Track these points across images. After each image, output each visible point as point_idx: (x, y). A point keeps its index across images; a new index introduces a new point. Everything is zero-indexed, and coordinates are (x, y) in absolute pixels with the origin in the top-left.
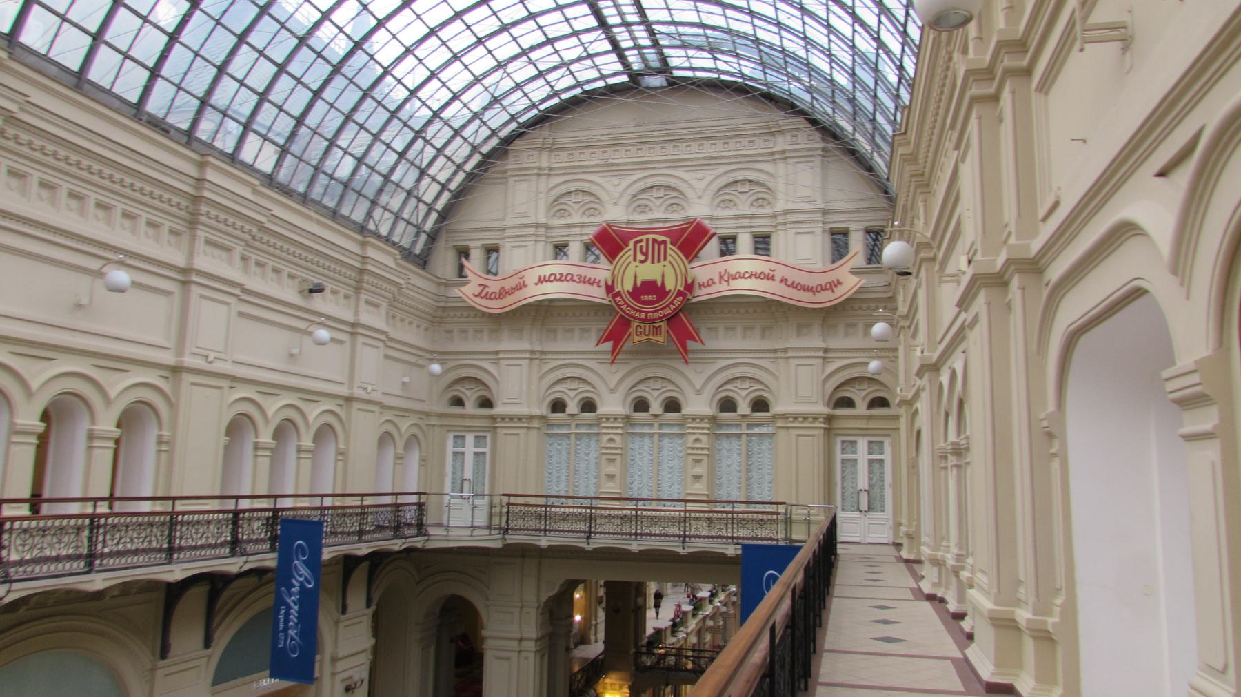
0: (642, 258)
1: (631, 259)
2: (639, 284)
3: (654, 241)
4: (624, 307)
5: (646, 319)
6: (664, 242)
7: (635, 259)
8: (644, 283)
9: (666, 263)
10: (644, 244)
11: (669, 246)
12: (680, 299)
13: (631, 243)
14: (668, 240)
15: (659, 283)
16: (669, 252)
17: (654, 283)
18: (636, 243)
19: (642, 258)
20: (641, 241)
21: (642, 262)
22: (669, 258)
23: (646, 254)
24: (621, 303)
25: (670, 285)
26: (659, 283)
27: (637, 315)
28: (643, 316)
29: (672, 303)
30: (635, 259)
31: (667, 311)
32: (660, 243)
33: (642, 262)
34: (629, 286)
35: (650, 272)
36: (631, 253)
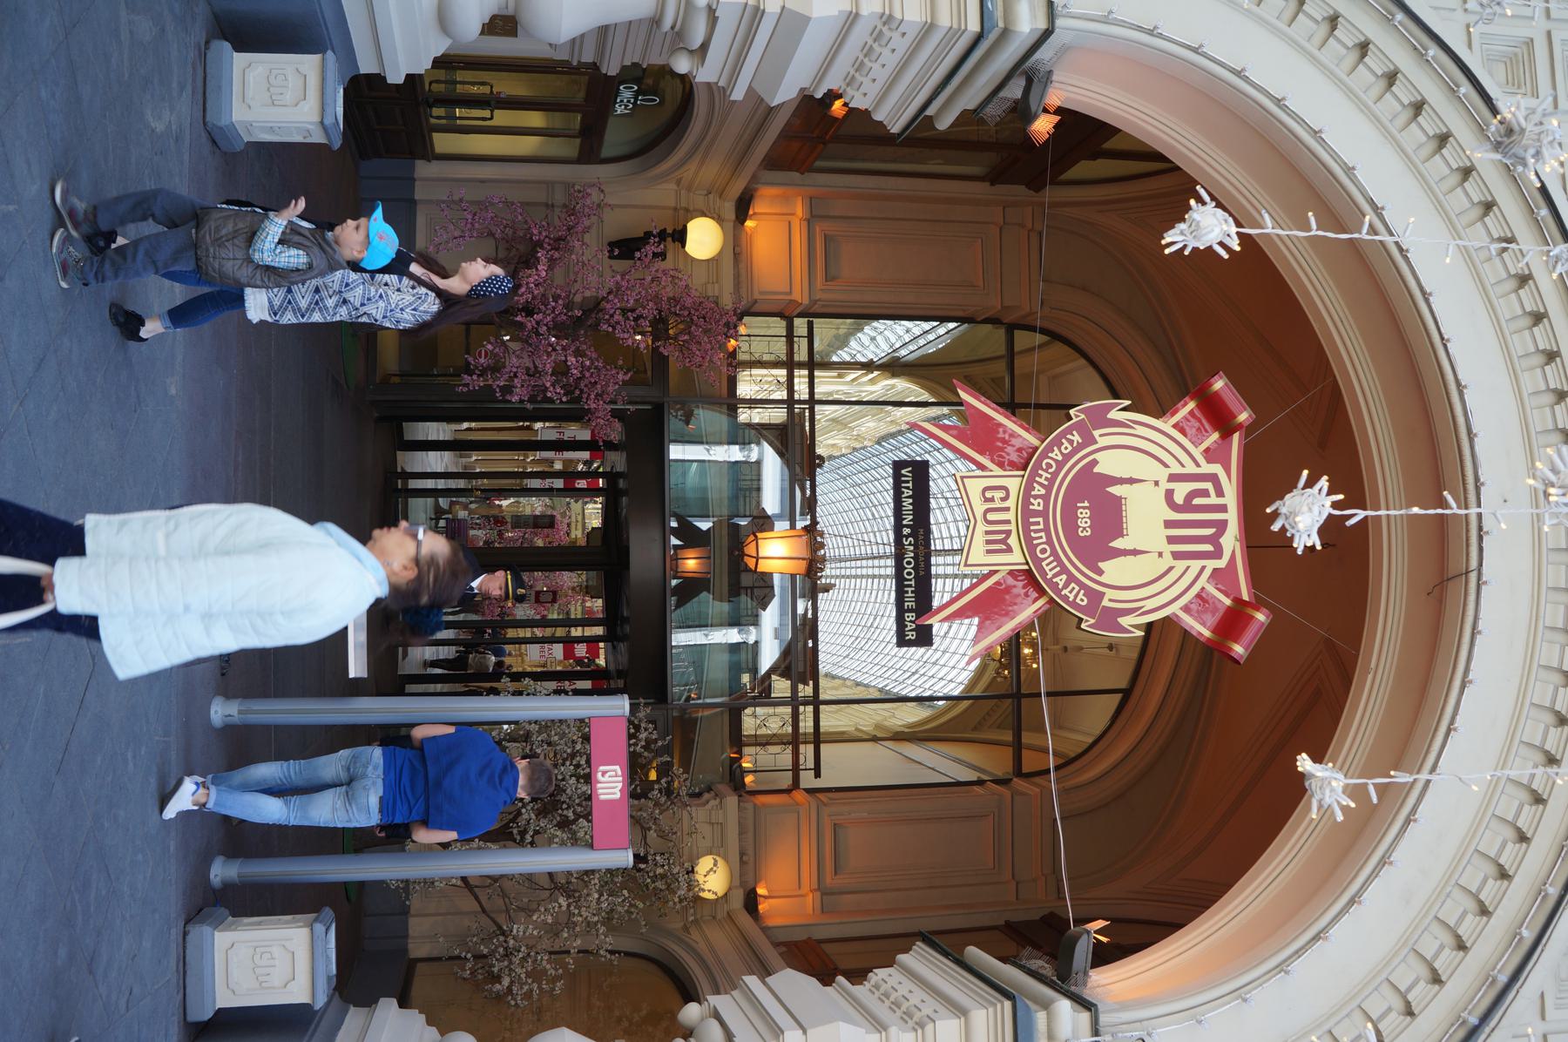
0: (1179, 499)
1: (1176, 469)
2: (1115, 490)
3: (1222, 526)
4: (1056, 454)
5: (1027, 513)
6: (1217, 554)
7: (1173, 478)
8: (1117, 502)
9: (1168, 561)
10: (1213, 500)
11: (1212, 564)
12: (1082, 600)
13: (1217, 469)
14: (1221, 563)
15: (1118, 544)
16: (1196, 565)
17: (1119, 532)
18: (1213, 478)
19: (1179, 499)
20: (1220, 493)
21: (1169, 494)
22: (1181, 565)
23: (1187, 507)
24: (1066, 447)
25: (1113, 571)
26: (1118, 544)
27: (1039, 490)
28: (1037, 505)
29: (1071, 579)
30: (1173, 478)
31: (1050, 569)
32: (1214, 540)
33: (1169, 494)
34: (1108, 464)
35: (1145, 517)
36: (1191, 469)
